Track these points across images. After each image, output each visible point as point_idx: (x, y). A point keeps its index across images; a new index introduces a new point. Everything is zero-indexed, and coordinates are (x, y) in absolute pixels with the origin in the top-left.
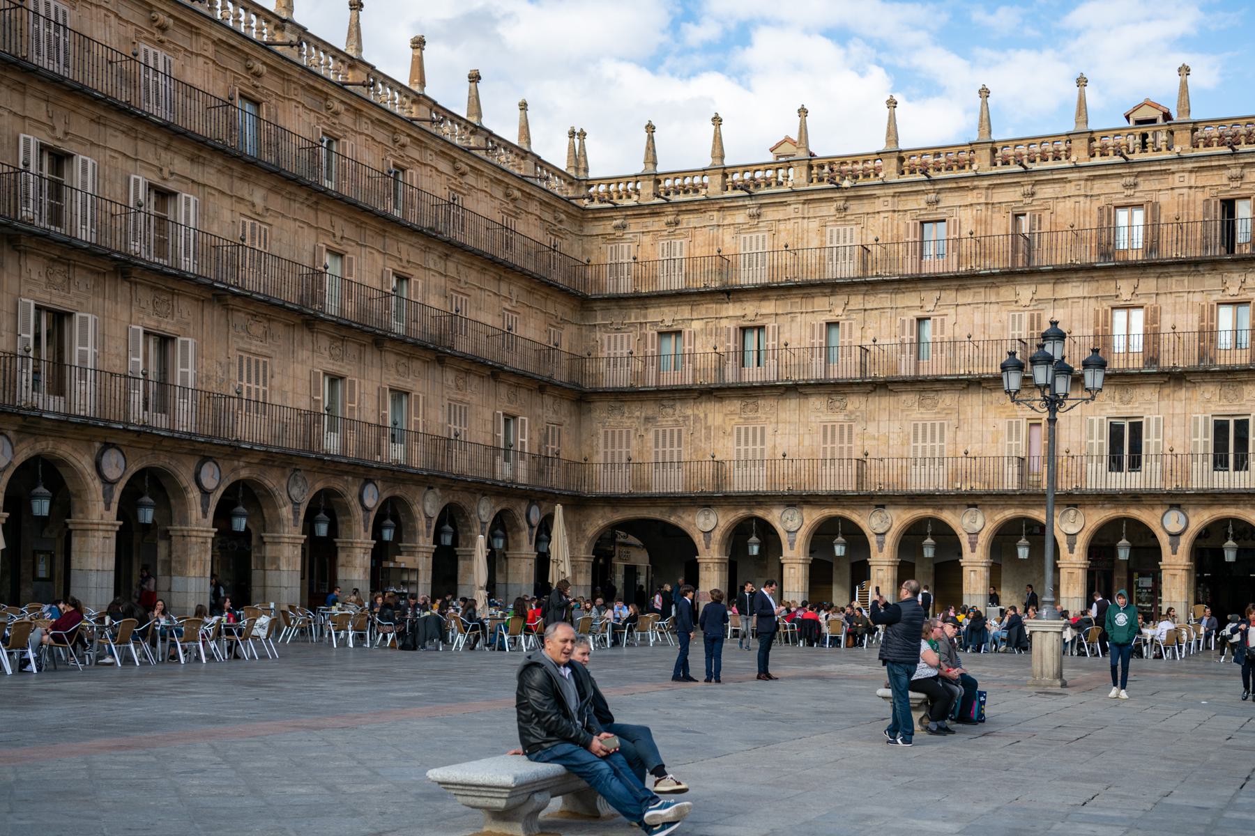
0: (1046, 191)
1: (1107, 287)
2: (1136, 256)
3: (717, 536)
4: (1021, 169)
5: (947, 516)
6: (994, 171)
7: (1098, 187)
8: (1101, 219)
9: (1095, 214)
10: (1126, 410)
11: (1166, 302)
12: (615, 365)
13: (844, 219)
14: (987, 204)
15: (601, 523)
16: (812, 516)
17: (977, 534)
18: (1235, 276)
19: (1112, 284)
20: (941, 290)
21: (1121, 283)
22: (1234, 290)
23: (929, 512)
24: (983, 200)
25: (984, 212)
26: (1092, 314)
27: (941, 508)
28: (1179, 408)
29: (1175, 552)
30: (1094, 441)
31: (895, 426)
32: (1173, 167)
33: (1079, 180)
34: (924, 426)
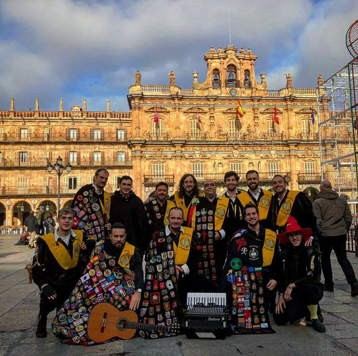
0: (53, 124)
2: (75, 140)
4: (47, 118)
5: (28, 200)
6: (40, 118)
7: (66, 124)
8: (66, 131)
9: (65, 130)
10: (73, 175)
11: (82, 151)
18: (97, 146)
19: (69, 146)
22: (97, 149)
23: (23, 200)
24: (37, 125)
26: (64, 153)
31: (14, 178)
32: (83, 121)
34: (21, 178)
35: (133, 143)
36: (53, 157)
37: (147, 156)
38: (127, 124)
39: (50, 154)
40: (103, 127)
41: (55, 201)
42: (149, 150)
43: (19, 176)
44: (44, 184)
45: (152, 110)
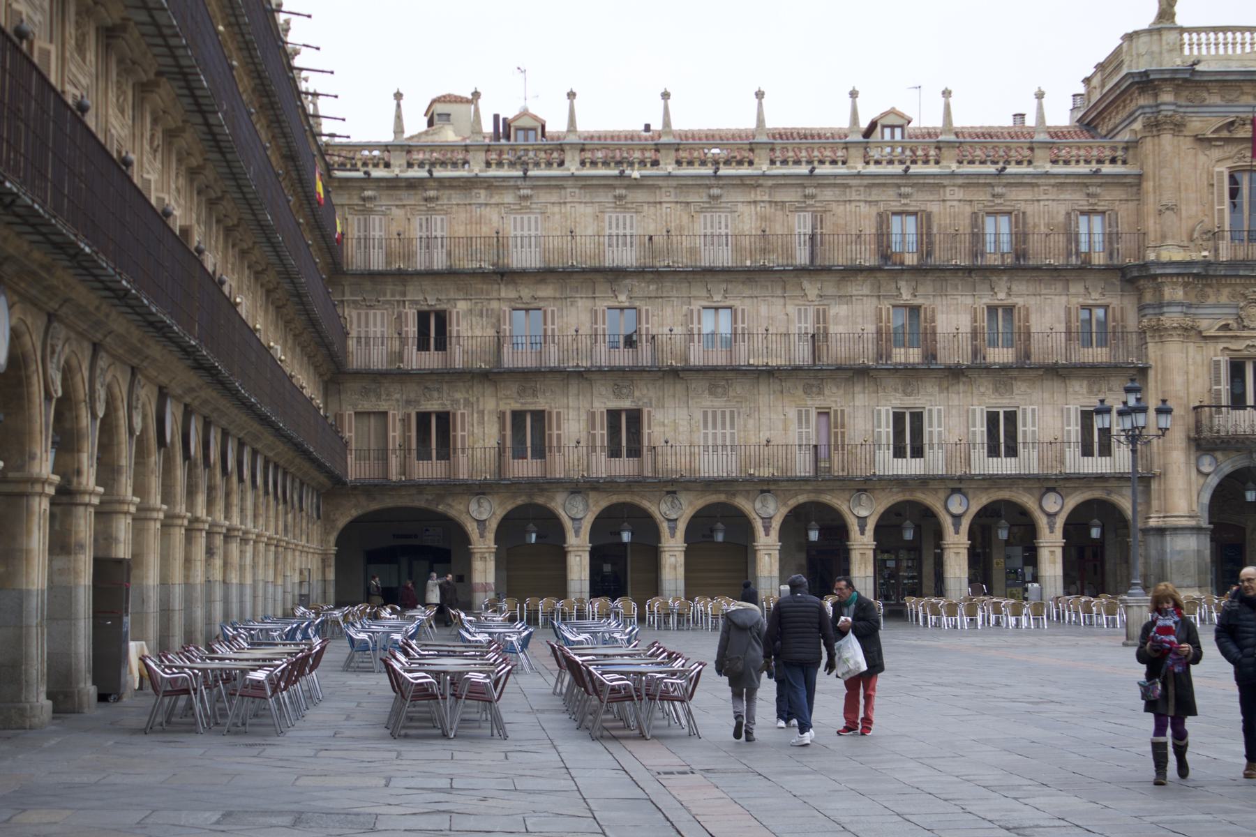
1: (888, 288)
2: (911, 260)
3: (493, 525)
5: (742, 503)
7: (875, 195)
12: (367, 344)
13: (625, 209)
14: (770, 202)
15: (354, 513)
16: (599, 504)
17: (771, 518)
20: (727, 281)
21: (902, 284)
23: (722, 498)
24: (766, 198)
25: (769, 210)
27: (734, 495)
28: (955, 400)
29: (957, 532)
30: (882, 430)
32: (945, 182)
33: (859, 186)
35: (1159, 272)
36: (832, 329)
37: (1204, 324)
38: (1118, 193)
39: (821, 317)
40: (1022, 206)
41: (840, 503)
42: (1211, 300)
43: (708, 402)
44: (800, 439)
45: (1225, 134)
